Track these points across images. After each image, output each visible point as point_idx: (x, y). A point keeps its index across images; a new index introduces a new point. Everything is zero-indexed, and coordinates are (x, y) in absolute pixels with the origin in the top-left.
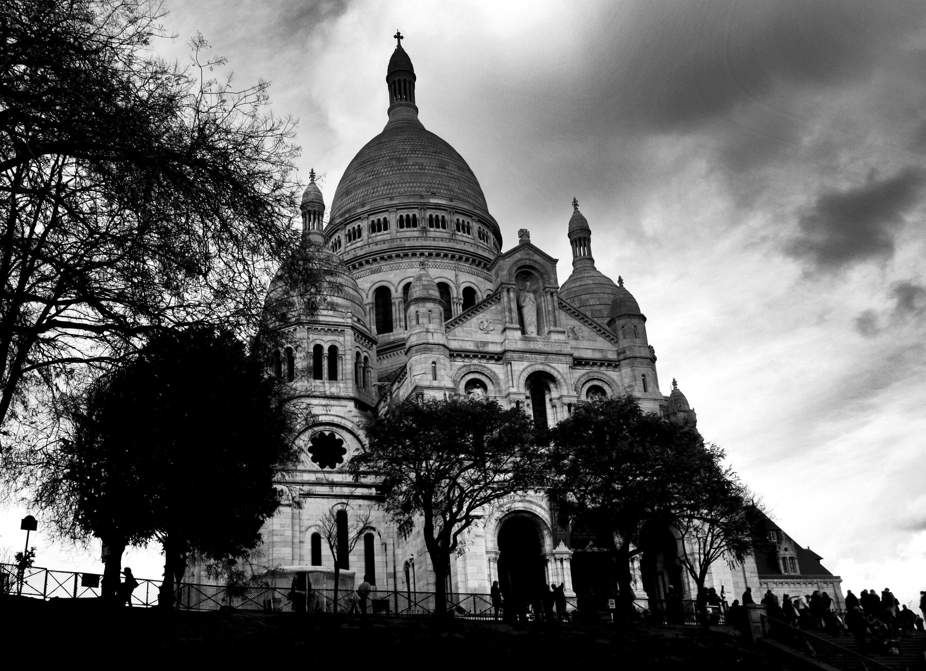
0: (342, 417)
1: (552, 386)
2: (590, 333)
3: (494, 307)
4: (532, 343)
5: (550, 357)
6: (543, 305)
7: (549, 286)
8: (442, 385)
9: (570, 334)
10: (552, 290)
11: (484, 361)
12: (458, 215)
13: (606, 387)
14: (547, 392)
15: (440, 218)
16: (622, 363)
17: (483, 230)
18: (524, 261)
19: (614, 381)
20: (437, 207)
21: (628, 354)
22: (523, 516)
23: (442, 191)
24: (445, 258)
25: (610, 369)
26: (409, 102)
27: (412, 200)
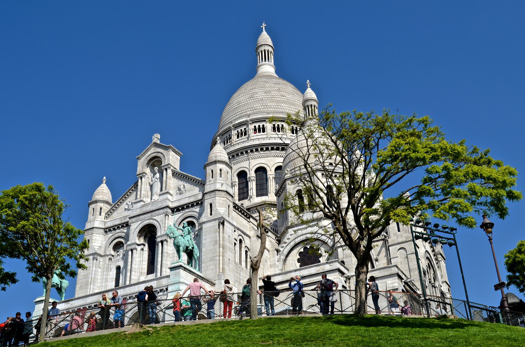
8: (90, 253)
9: (178, 192)
16: (203, 199)
17: (278, 125)
18: (151, 155)
24: (243, 155)
26: (264, 62)
27: (227, 127)
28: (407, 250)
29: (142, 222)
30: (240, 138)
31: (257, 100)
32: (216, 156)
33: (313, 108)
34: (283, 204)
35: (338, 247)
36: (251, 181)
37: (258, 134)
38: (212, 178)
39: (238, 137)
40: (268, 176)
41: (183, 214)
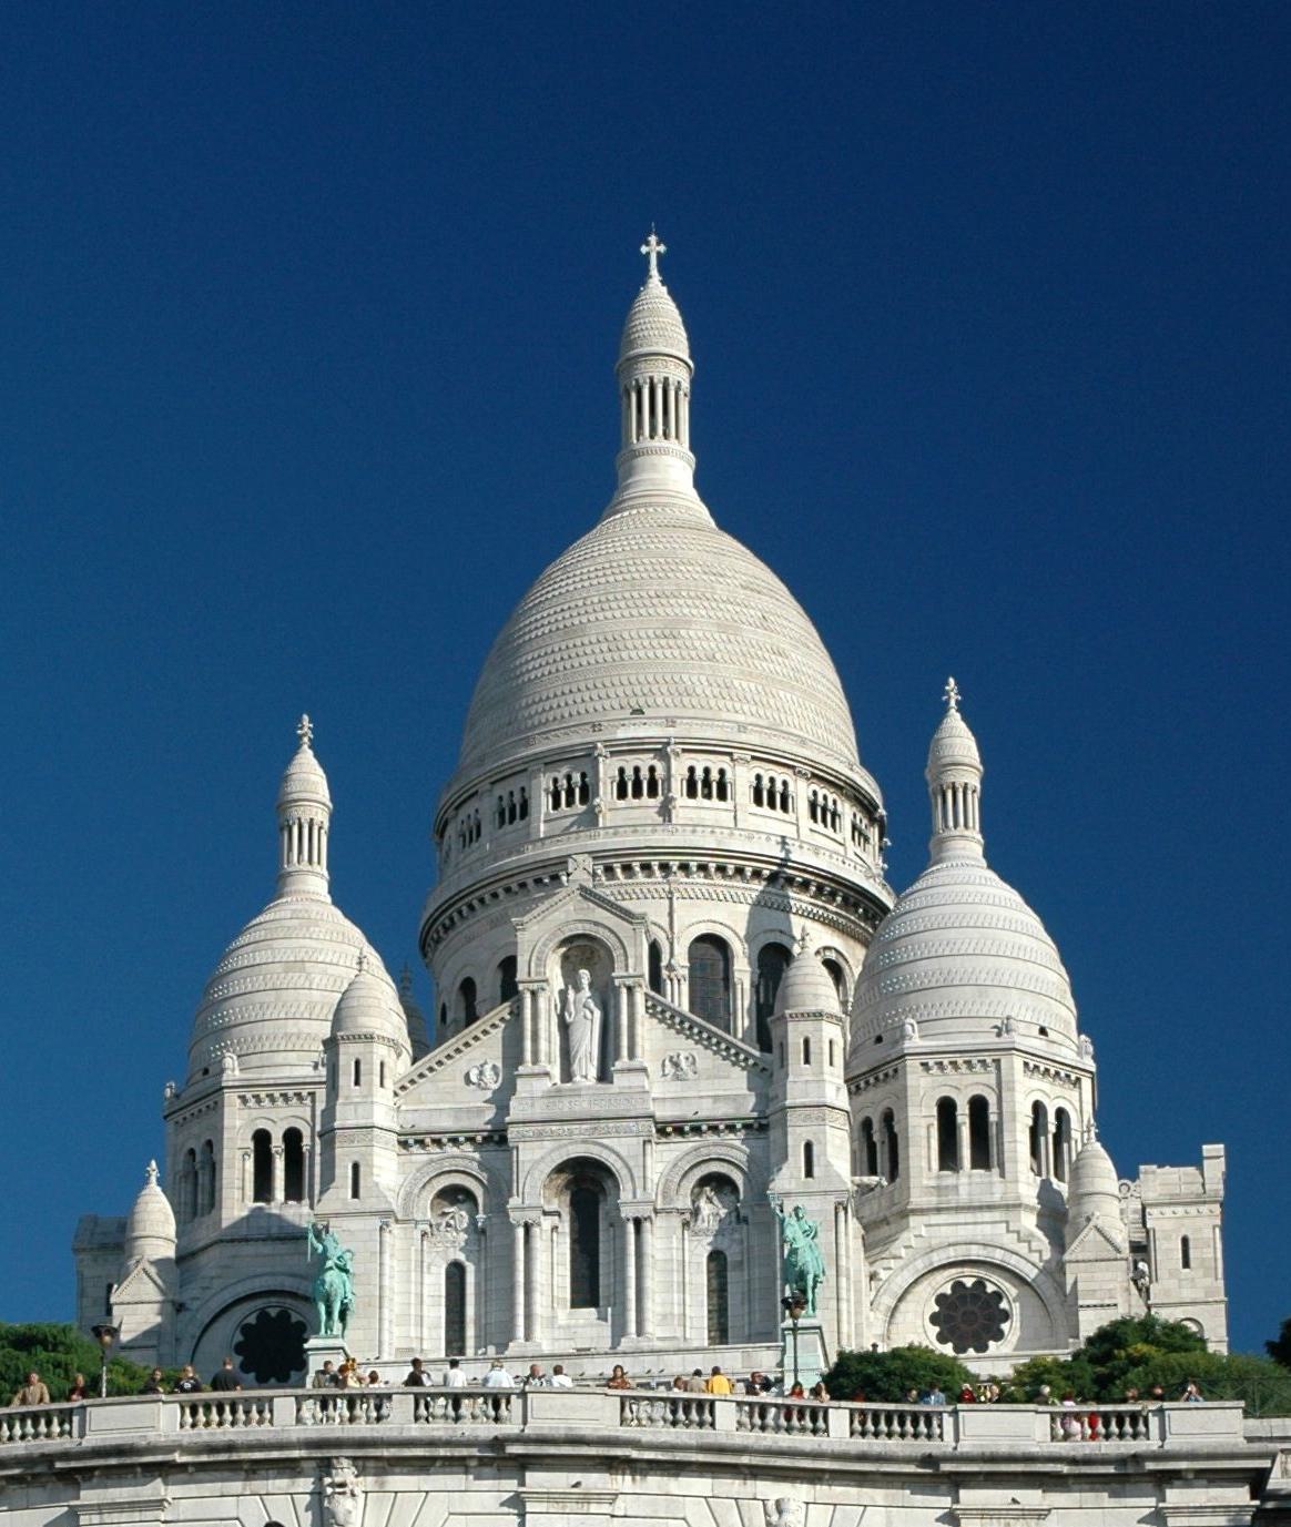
0: (302, 1277)
1: (609, 1184)
4: (566, 1101)
5: (602, 1125)
9: (669, 1069)
10: (629, 982)
14: (601, 1198)
15: (644, 774)
16: (772, 1118)
17: (772, 780)
20: (634, 747)
23: (659, 701)
27: (576, 740)
28: (1205, 1328)
29: (560, 1147)
30: (630, 800)
31: (693, 654)
33: (969, 792)
34: (876, 1126)
35: (1081, 1306)
36: (676, 982)
37: (700, 801)
38: (807, 1061)
39: (622, 794)
40: (737, 975)
41: (695, 1150)
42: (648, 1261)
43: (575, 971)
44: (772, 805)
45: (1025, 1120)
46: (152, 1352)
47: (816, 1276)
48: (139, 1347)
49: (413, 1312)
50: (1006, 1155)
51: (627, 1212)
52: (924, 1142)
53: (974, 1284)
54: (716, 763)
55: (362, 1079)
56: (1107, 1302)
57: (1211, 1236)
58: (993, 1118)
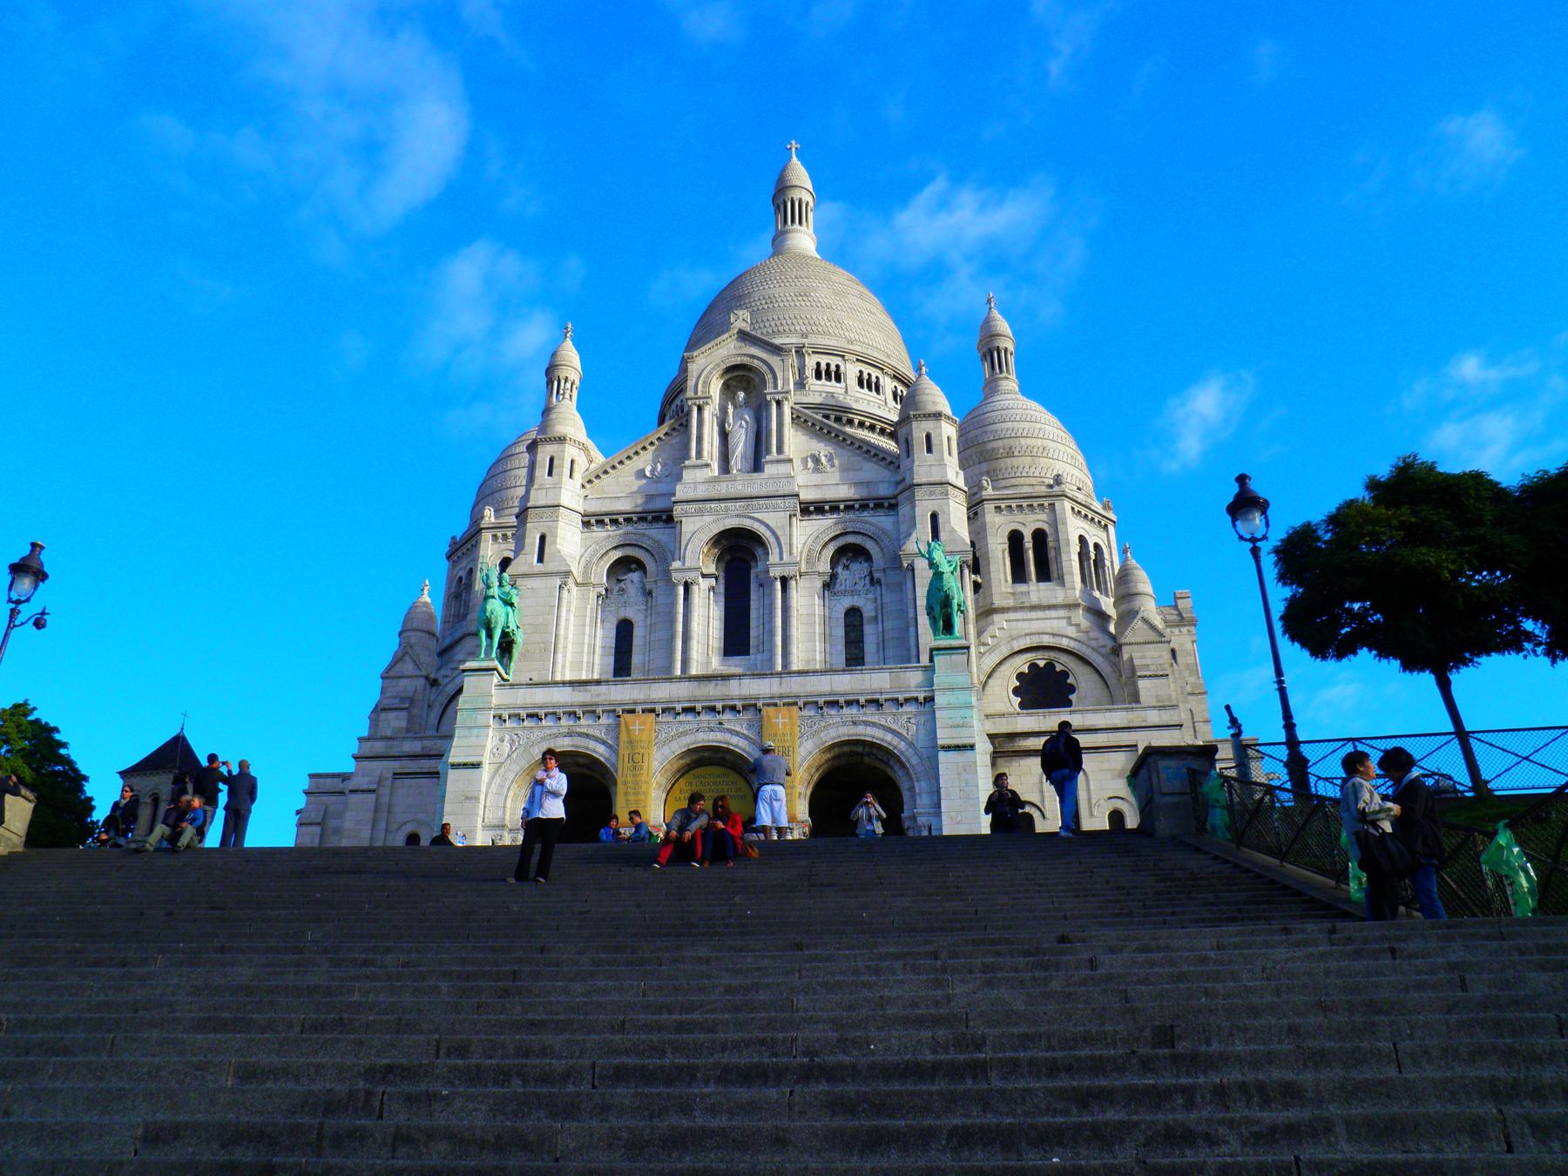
1: (759, 552)
2: (851, 459)
3: (674, 442)
6: (764, 425)
7: (773, 391)
9: (810, 464)
11: (642, 527)
12: (817, 355)
13: (870, 545)
14: (753, 564)
16: (901, 498)
17: (869, 375)
19: (885, 532)
21: (908, 482)
22: (578, 765)
25: (880, 512)
32: (933, 403)
35: (1140, 677)
38: (929, 450)
42: (794, 613)
43: (733, 398)
44: (869, 388)
45: (1075, 548)
46: (404, 714)
47: (959, 605)
48: (396, 709)
49: (585, 659)
50: (1064, 570)
51: (775, 572)
52: (1001, 562)
53: (1045, 665)
54: (834, 361)
55: (555, 470)
56: (1161, 673)
57: (1192, 648)
58: (1051, 544)
